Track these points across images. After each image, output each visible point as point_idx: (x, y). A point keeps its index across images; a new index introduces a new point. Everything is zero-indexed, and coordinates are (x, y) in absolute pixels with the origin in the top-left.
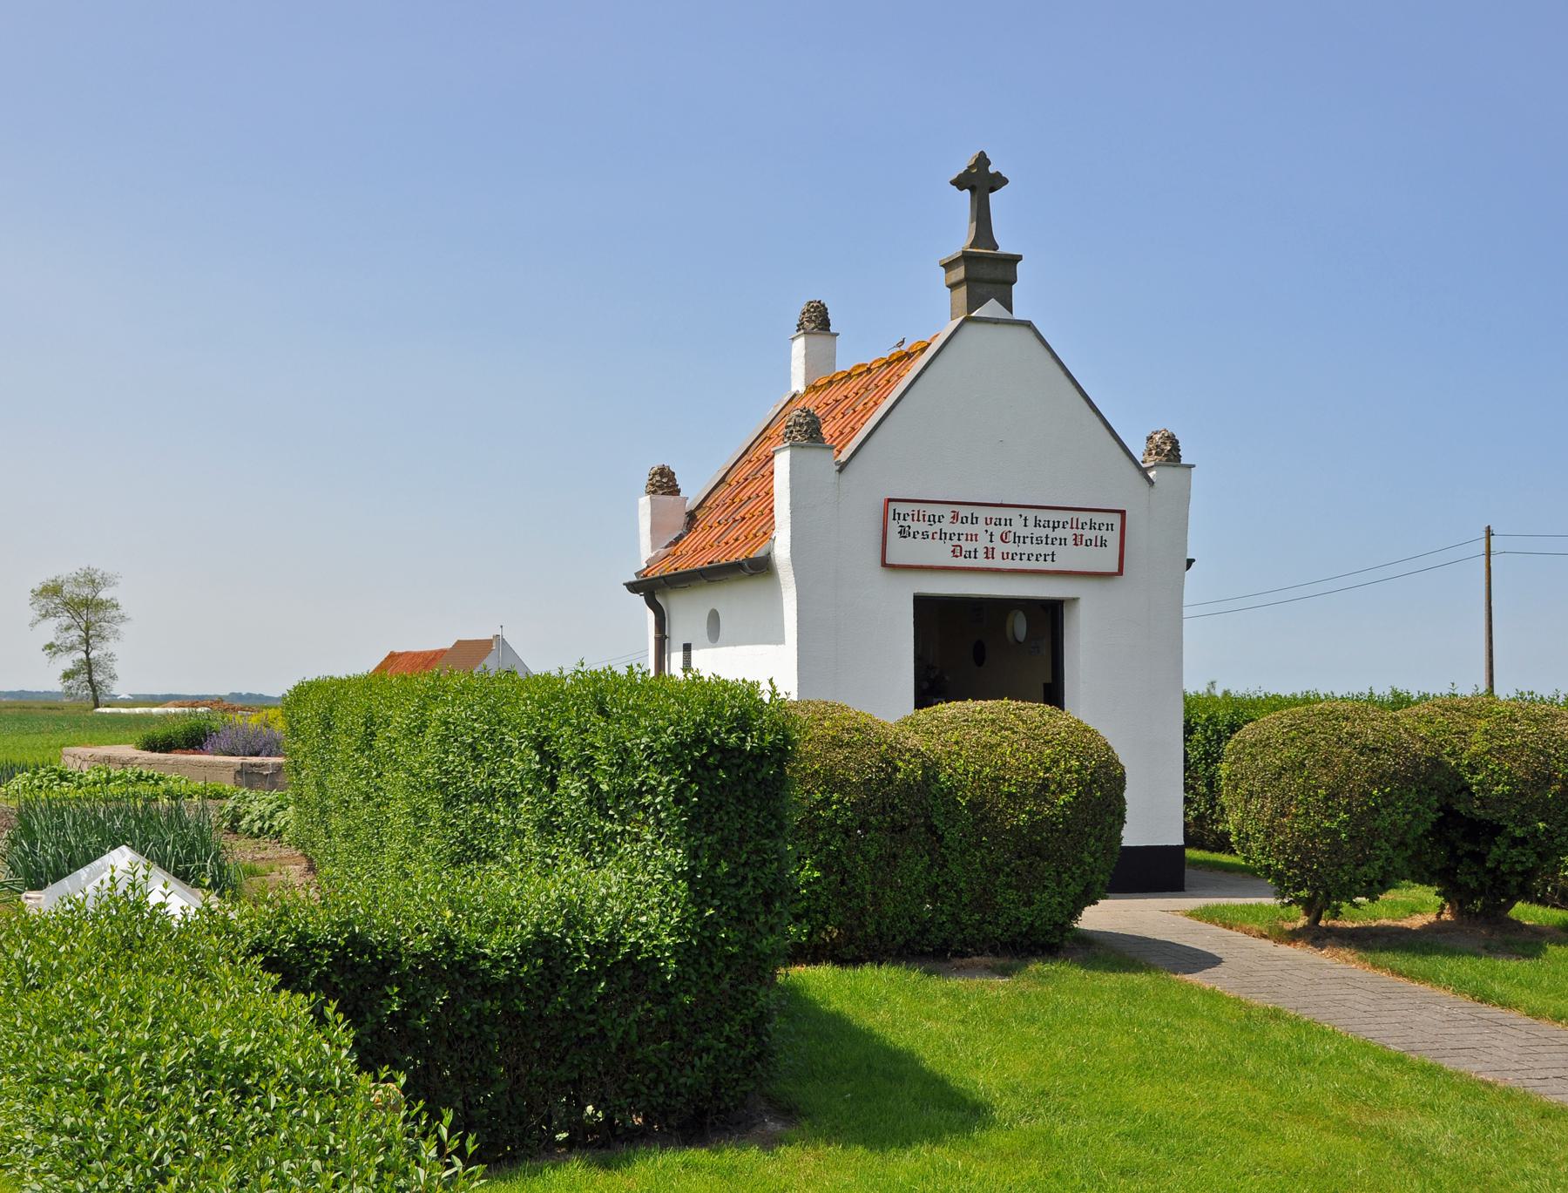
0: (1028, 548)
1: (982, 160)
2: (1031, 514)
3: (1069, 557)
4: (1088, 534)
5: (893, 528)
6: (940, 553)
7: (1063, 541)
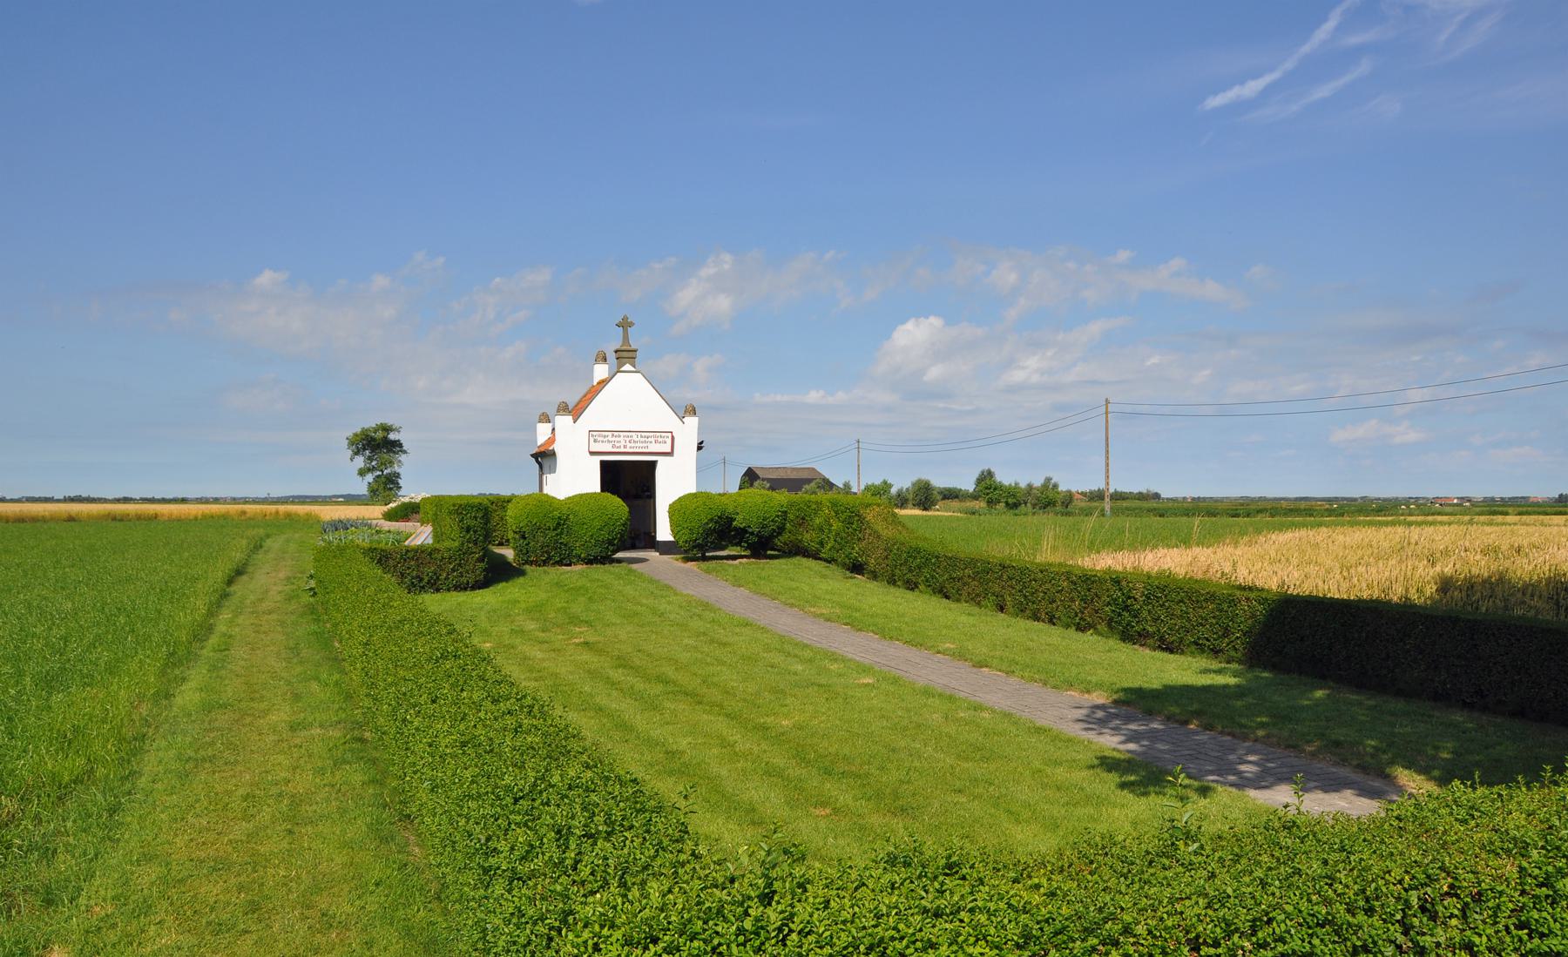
1: (625, 319)
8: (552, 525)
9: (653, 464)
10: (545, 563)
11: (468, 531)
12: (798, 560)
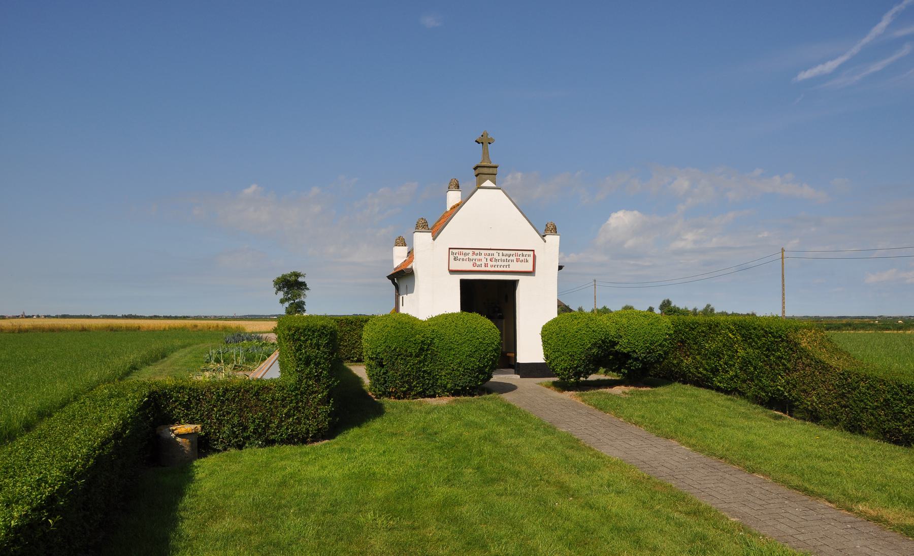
0: (500, 263)
2: (501, 252)
3: (515, 267)
4: (521, 258)
5: (452, 257)
6: (468, 266)
7: (512, 261)
8: (413, 350)
9: (514, 284)
10: (405, 395)
11: (307, 363)
12: (677, 386)
